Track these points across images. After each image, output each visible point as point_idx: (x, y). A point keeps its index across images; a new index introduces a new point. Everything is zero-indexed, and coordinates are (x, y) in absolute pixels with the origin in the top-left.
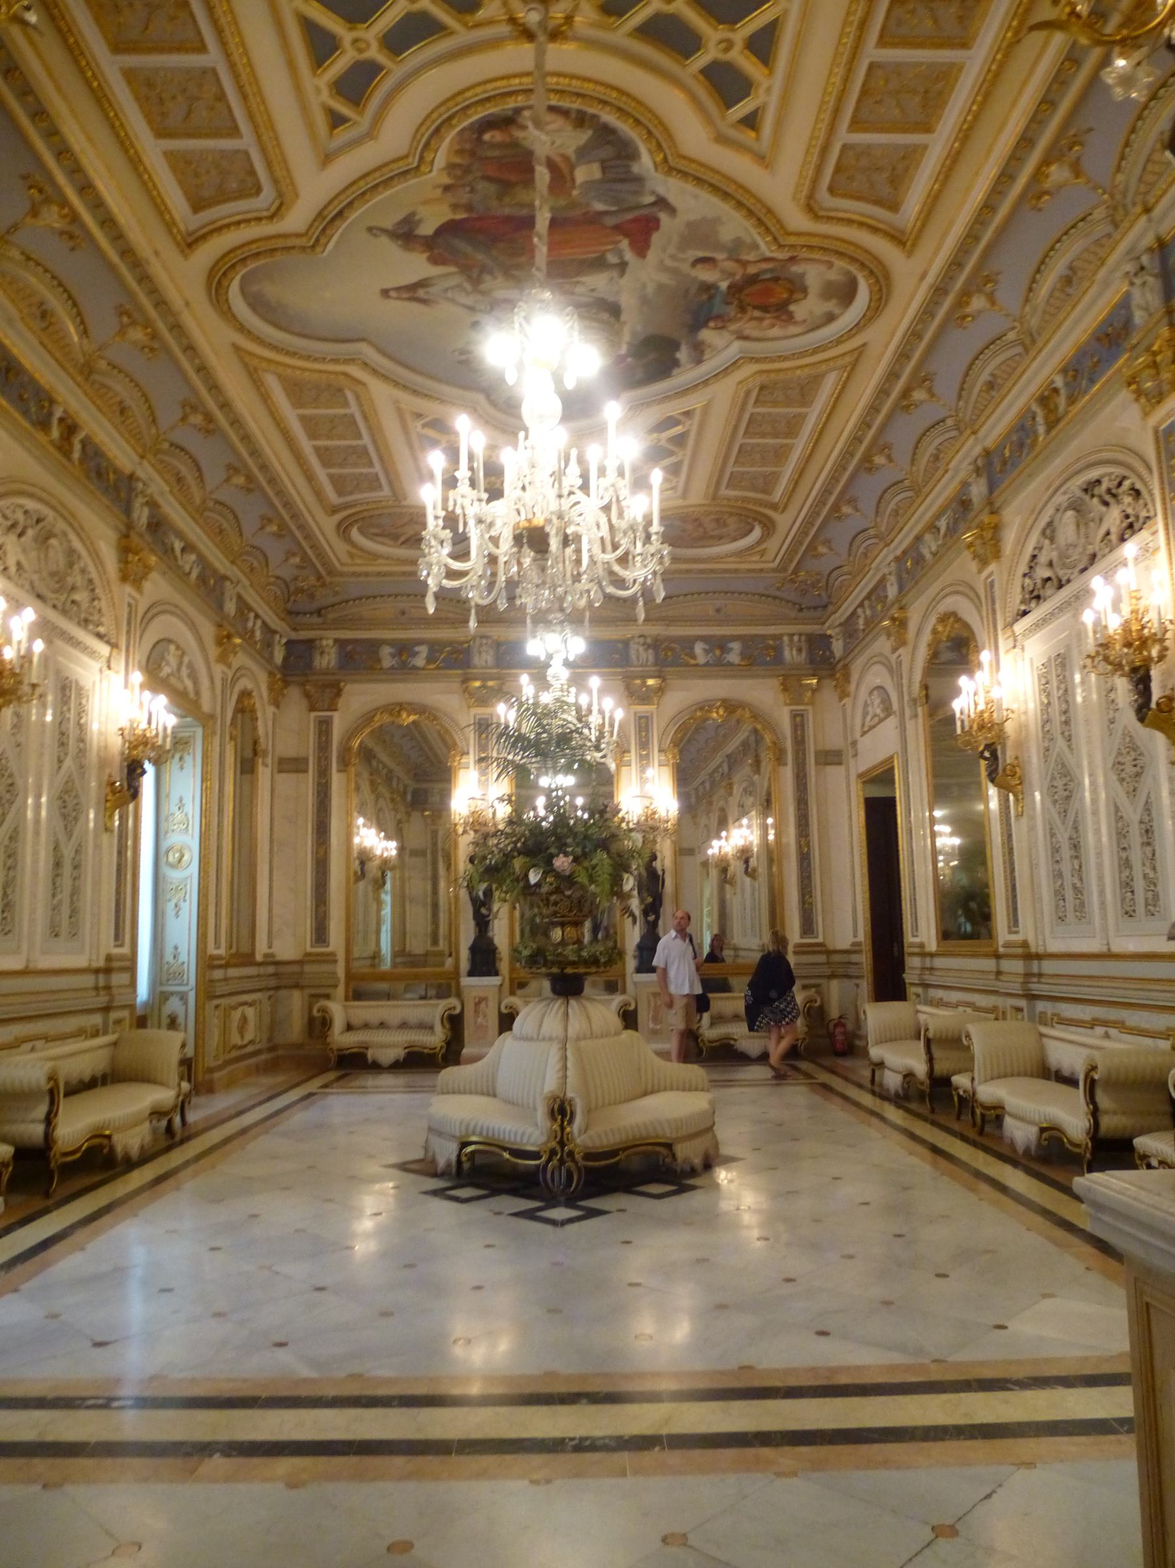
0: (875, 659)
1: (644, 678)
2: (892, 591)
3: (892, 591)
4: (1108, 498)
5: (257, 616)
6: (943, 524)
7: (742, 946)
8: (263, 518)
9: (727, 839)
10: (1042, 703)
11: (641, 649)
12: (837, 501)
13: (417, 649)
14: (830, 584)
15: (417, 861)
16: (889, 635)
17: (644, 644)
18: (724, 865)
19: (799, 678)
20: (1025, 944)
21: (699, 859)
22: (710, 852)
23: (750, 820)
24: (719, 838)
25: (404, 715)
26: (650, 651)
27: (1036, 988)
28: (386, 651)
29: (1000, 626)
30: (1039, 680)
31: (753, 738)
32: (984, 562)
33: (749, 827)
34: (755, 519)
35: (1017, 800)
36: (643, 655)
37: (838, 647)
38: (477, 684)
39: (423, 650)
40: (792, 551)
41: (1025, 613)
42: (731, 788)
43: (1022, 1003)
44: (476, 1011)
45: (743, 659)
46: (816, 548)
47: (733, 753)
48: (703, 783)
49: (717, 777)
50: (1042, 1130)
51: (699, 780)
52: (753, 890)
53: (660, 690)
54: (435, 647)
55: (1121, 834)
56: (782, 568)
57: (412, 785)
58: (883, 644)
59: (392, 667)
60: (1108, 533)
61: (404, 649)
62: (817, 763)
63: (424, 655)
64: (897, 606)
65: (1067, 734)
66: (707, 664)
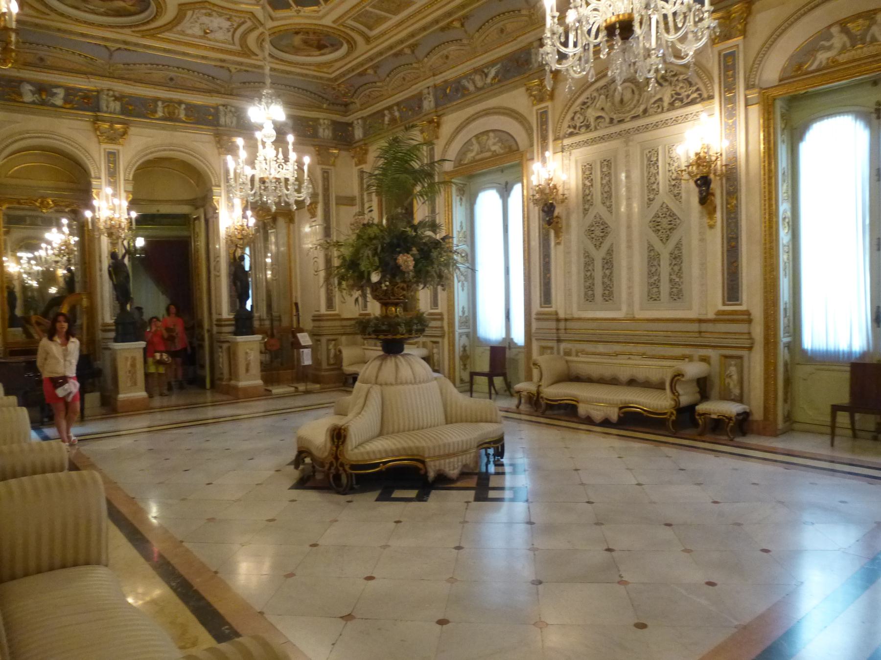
2: (428, 104)
4: (661, 81)
6: (493, 72)
10: (584, 185)
19: (328, 148)
20: (557, 314)
27: (563, 336)
30: (584, 173)
35: (557, 235)
37: (358, 133)
38: (106, 126)
41: (571, 134)
43: (553, 344)
50: (621, 408)
55: (653, 258)
59: (33, 103)
60: (661, 100)
62: (337, 204)
65: (608, 204)
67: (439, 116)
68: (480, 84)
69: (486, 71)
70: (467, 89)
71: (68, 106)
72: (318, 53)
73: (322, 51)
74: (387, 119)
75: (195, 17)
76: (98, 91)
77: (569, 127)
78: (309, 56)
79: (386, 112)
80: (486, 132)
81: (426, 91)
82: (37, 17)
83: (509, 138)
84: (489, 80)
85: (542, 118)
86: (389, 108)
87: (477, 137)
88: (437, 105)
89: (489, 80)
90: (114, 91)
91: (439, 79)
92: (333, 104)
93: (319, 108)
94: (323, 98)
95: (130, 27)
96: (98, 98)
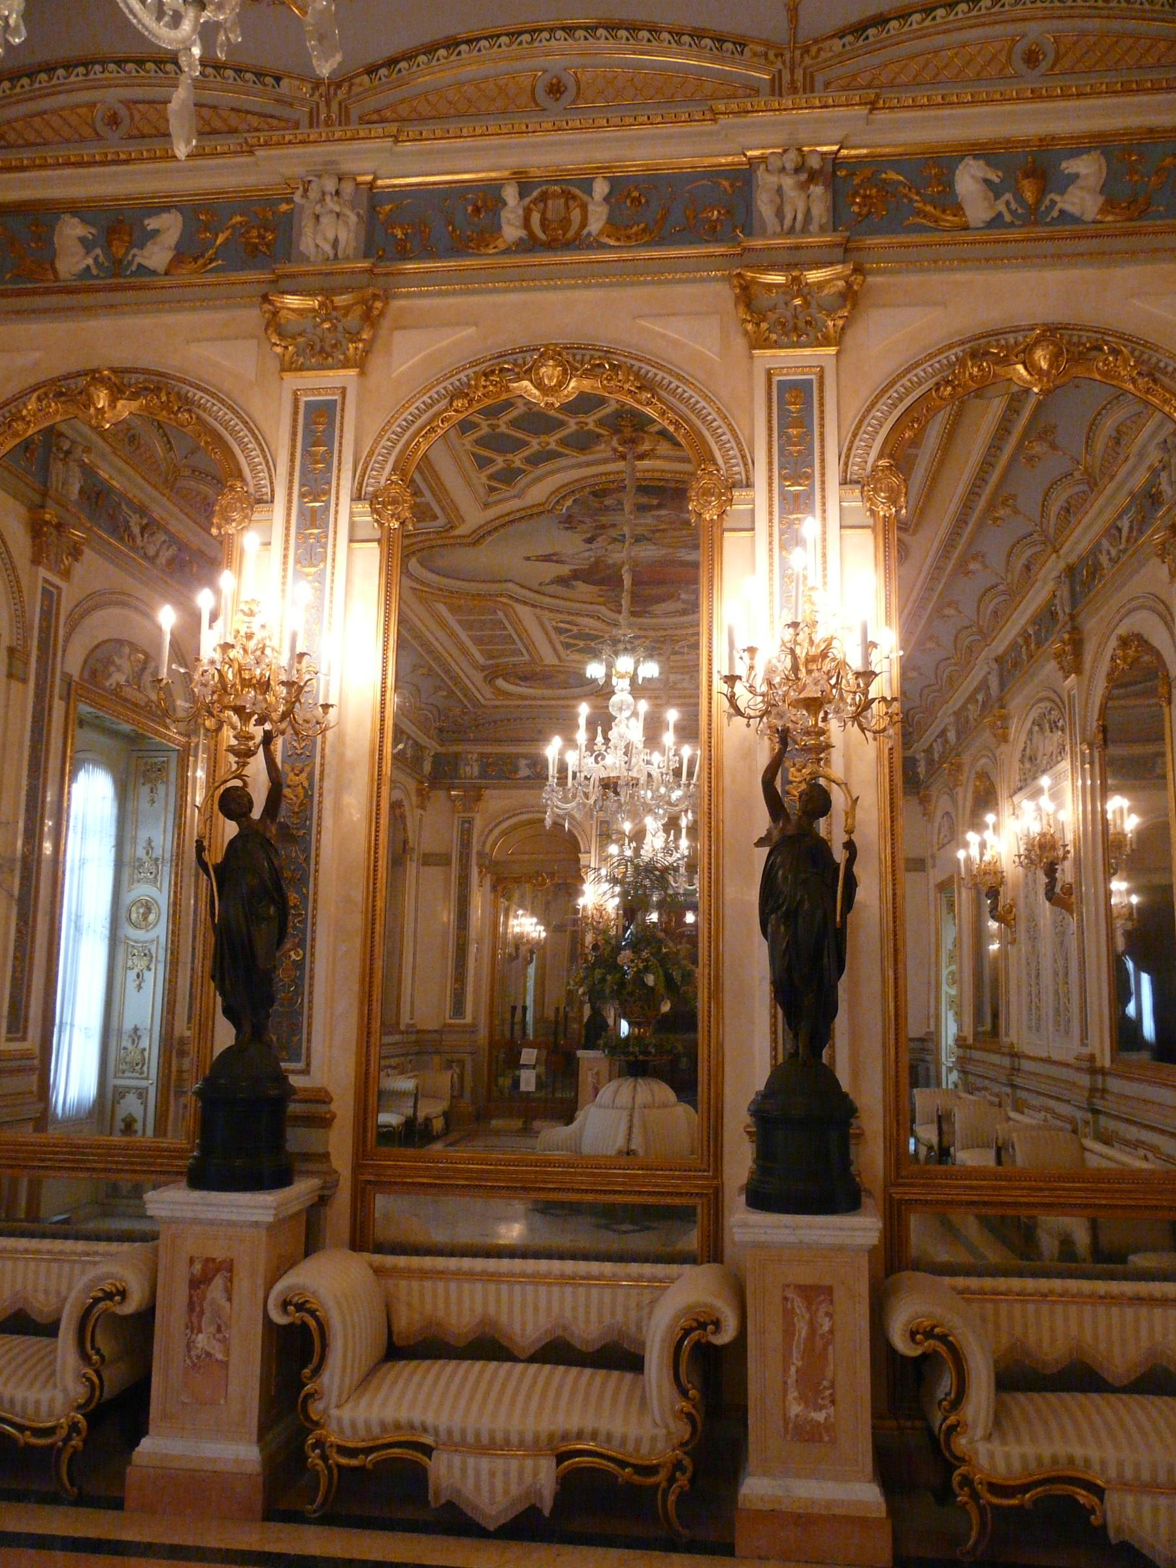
1: (794, 262)
7: (1028, 1050)
9: (996, 828)
11: (788, 182)
13: (152, 224)
15: (434, 873)
17: (797, 170)
18: (991, 880)
21: (936, 876)
22: (961, 854)
23: (1057, 779)
24: (979, 826)
25: (102, 399)
26: (817, 190)
28: (72, 230)
31: (1065, 592)
33: (1055, 796)
36: (795, 202)
39: (169, 227)
42: (1005, 728)
44: (194, 1307)
45: (1110, 205)
47: (1014, 645)
48: (943, 733)
49: (973, 711)
51: (935, 729)
52: (1061, 934)
53: (850, 298)
54: (201, 214)
57: (433, 746)
61: (119, 225)
66: (996, 222)
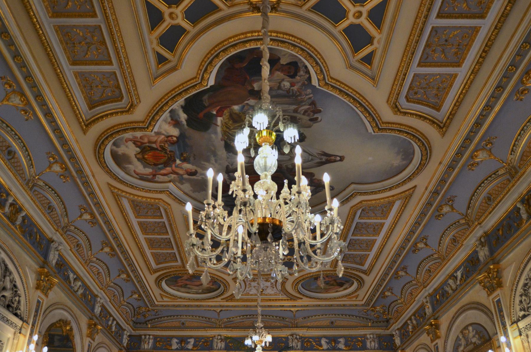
0: (420, 347)
2: (429, 310)
3: (429, 310)
5: (114, 319)
8: (119, 270)
12: (397, 267)
13: (189, 340)
14: (390, 310)
16: (428, 334)
28: (175, 341)
29: (508, 323)
32: (491, 290)
34: (354, 278)
37: (398, 341)
39: (192, 341)
40: (373, 295)
41: (524, 316)
46: (384, 293)
54: (197, 339)
56: (367, 304)
58: (425, 339)
59: (177, 349)
63: (192, 343)
64: (433, 318)
67: (435, 319)
68: (454, 287)
69: (455, 275)
70: (447, 292)
71: (195, 349)
72: (341, 289)
73: (344, 287)
74: (410, 327)
75: (247, 284)
76: (212, 337)
77: (521, 310)
78: (337, 291)
79: (409, 322)
80: (466, 328)
81: (425, 301)
82: (171, 302)
83: (484, 330)
84: (458, 282)
85: (498, 306)
86: (410, 319)
87: (462, 332)
88: (434, 309)
89: (458, 282)
90: (221, 336)
91: (430, 289)
92: (376, 322)
93: (365, 327)
94: (367, 319)
95: (217, 297)
96: (212, 341)
